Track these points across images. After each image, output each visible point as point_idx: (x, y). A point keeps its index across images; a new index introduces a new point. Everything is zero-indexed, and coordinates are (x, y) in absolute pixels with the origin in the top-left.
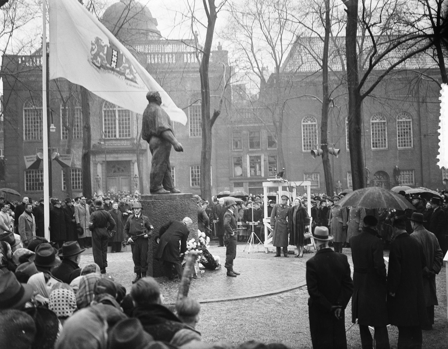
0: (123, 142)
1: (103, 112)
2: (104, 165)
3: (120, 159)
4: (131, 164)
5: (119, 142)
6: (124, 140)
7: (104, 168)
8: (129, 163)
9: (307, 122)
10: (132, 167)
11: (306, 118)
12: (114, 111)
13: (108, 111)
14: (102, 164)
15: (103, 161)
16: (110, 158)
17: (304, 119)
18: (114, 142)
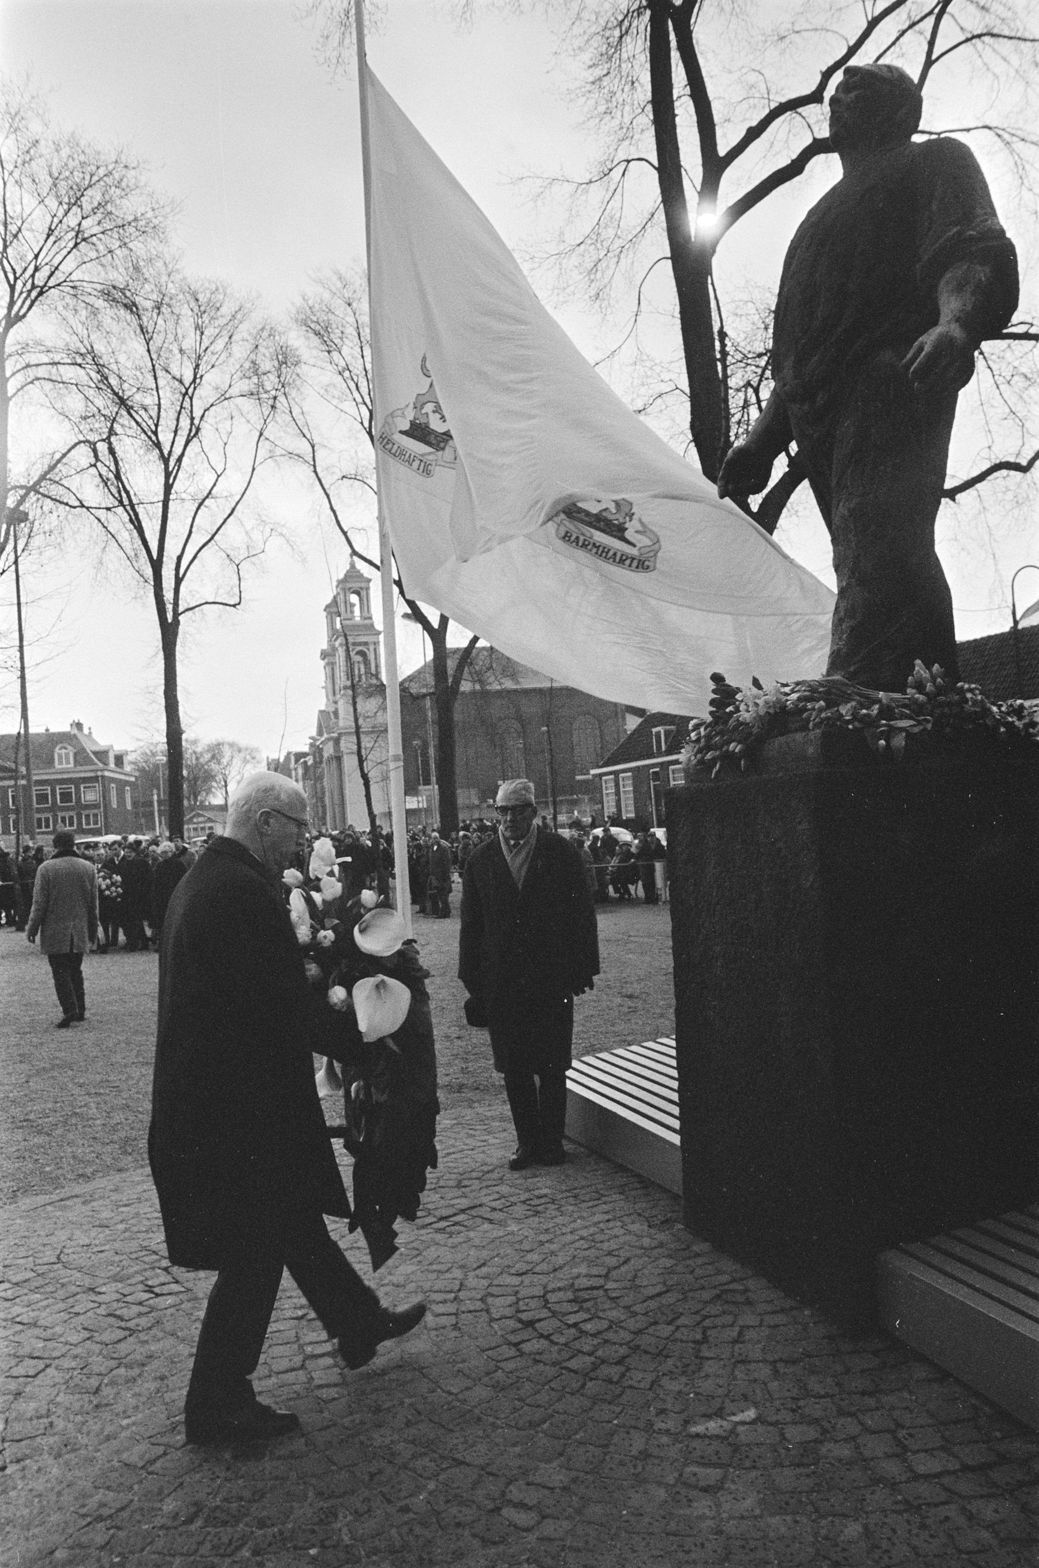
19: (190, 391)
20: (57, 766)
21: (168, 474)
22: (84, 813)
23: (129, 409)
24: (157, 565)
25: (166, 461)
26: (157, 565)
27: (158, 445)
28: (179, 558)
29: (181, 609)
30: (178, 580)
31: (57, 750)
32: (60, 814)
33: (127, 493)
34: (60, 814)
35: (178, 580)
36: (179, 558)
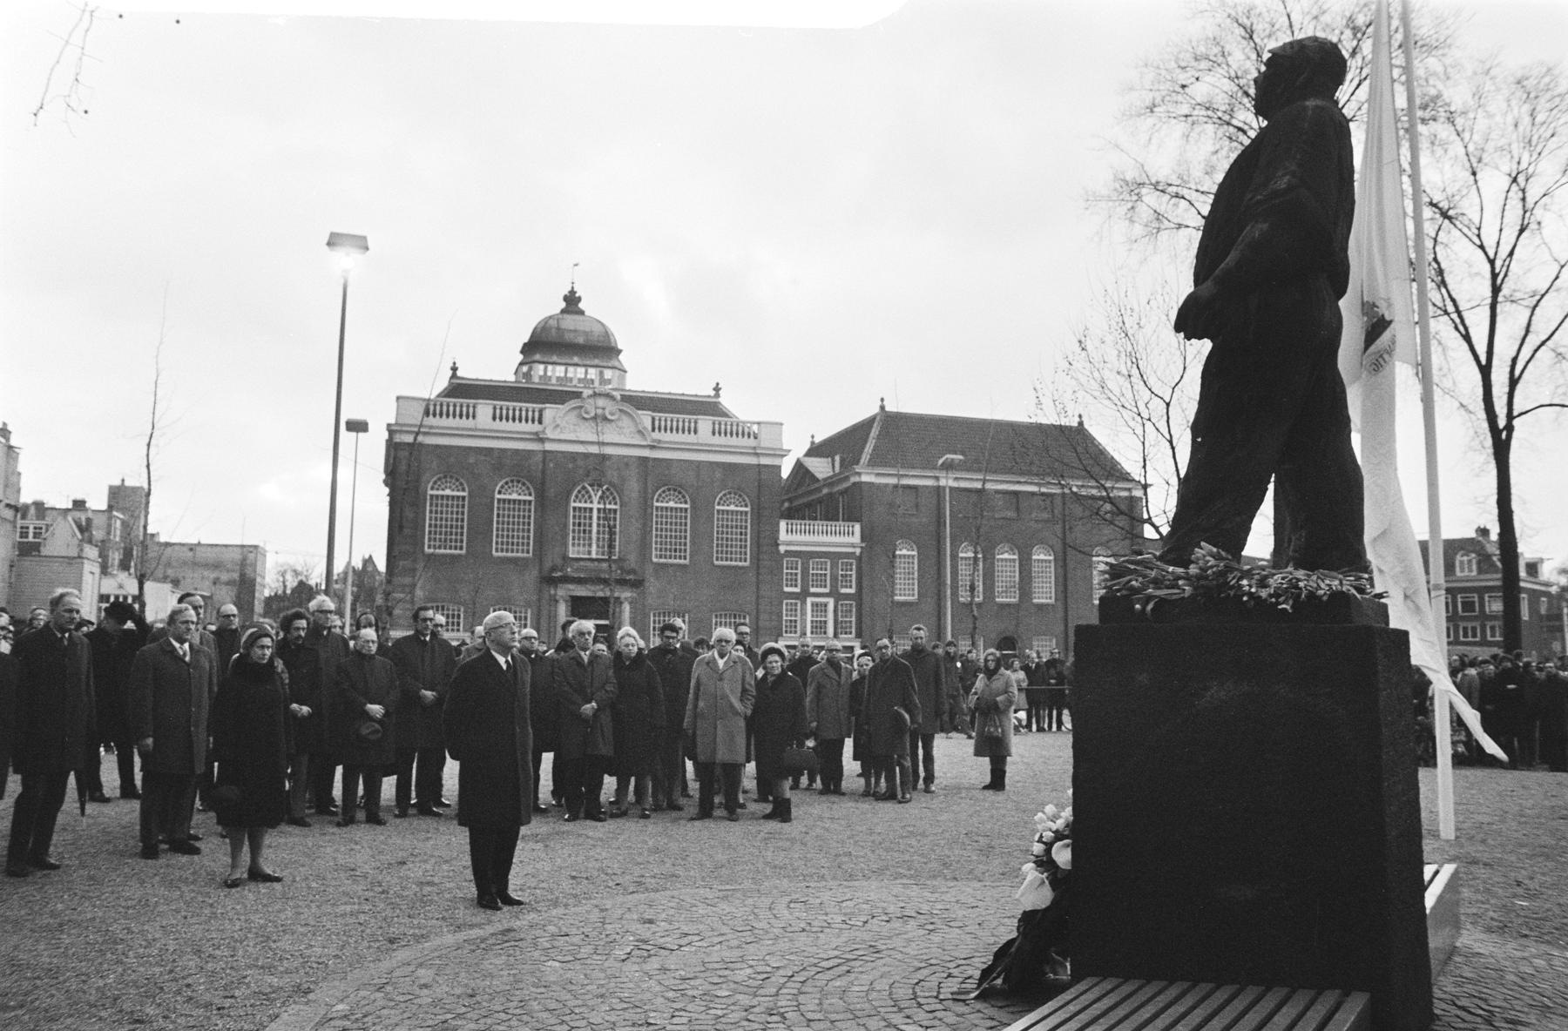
16: (581, 591)
18: (589, 564)
19: (1521, 179)
20: (1458, 573)
21: (1494, 276)
22: (1489, 624)
23: (1450, 218)
24: (1486, 371)
25: (1492, 262)
26: (1486, 371)
27: (1482, 247)
28: (1514, 360)
29: (1515, 413)
30: (1513, 382)
31: (1458, 557)
32: (1462, 625)
33: (1453, 300)
34: (1462, 625)
35: (1513, 382)
36: (1514, 360)
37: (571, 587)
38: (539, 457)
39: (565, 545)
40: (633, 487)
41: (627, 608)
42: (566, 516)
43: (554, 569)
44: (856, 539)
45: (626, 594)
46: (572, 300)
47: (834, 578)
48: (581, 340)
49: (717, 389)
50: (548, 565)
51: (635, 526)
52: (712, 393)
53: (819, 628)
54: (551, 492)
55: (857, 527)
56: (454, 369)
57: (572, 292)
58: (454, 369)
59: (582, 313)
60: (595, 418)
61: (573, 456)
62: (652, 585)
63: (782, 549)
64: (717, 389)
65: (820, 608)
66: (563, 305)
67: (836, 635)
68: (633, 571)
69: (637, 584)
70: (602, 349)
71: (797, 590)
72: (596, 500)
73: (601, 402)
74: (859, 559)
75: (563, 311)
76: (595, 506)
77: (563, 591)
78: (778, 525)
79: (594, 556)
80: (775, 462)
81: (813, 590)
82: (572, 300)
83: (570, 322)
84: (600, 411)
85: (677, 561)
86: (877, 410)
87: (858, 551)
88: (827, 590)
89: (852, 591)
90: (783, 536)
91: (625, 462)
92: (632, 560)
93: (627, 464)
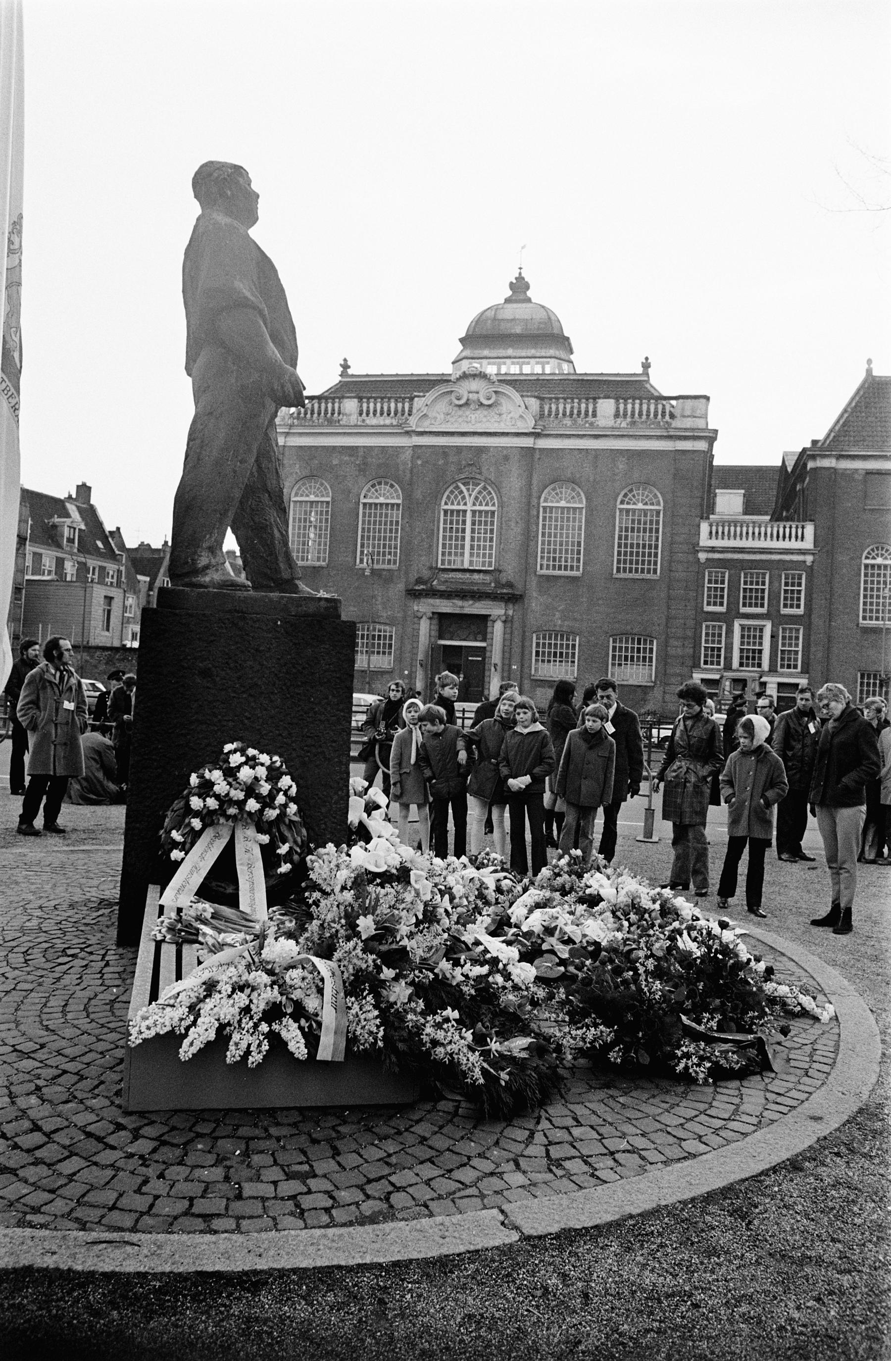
0: (476, 576)
1: (442, 513)
2: (435, 622)
3: (467, 611)
4: (490, 624)
5: (468, 575)
6: (479, 571)
7: (435, 627)
8: (484, 618)
9: (874, 558)
10: (489, 630)
11: (873, 550)
12: (465, 511)
13: (452, 511)
14: (430, 618)
15: (433, 613)
16: (446, 606)
17: (869, 553)
18: (459, 575)
37: (438, 601)
38: (409, 453)
39: (431, 550)
40: (514, 483)
41: (498, 630)
42: (435, 521)
43: (419, 581)
44: (808, 543)
45: (496, 610)
46: (520, 287)
47: (774, 597)
48: (518, 330)
49: (646, 366)
50: (414, 576)
51: (515, 531)
52: (640, 370)
53: (751, 657)
54: (418, 494)
55: (809, 529)
56: (345, 366)
57: (520, 278)
58: (345, 366)
59: (529, 300)
60: (467, 404)
61: (444, 451)
62: (536, 602)
63: (702, 556)
64: (646, 366)
65: (752, 635)
66: (509, 293)
67: (773, 670)
68: (510, 585)
69: (513, 598)
70: (550, 337)
71: (723, 609)
72: (470, 501)
73: (474, 385)
74: (810, 571)
75: (508, 301)
76: (469, 507)
77: (426, 606)
78: (699, 526)
79: (466, 565)
80: (702, 445)
81: (743, 610)
82: (520, 287)
83: (519, 311)
84: (473, 397)
85: (568, 573)
86: (862, 376)
87: (809, 559)
88: (764, 610)
89: (801, 611)
90: (704, 541)
91: (505, 455)
92: (510, 572)
93: (506, 458)
